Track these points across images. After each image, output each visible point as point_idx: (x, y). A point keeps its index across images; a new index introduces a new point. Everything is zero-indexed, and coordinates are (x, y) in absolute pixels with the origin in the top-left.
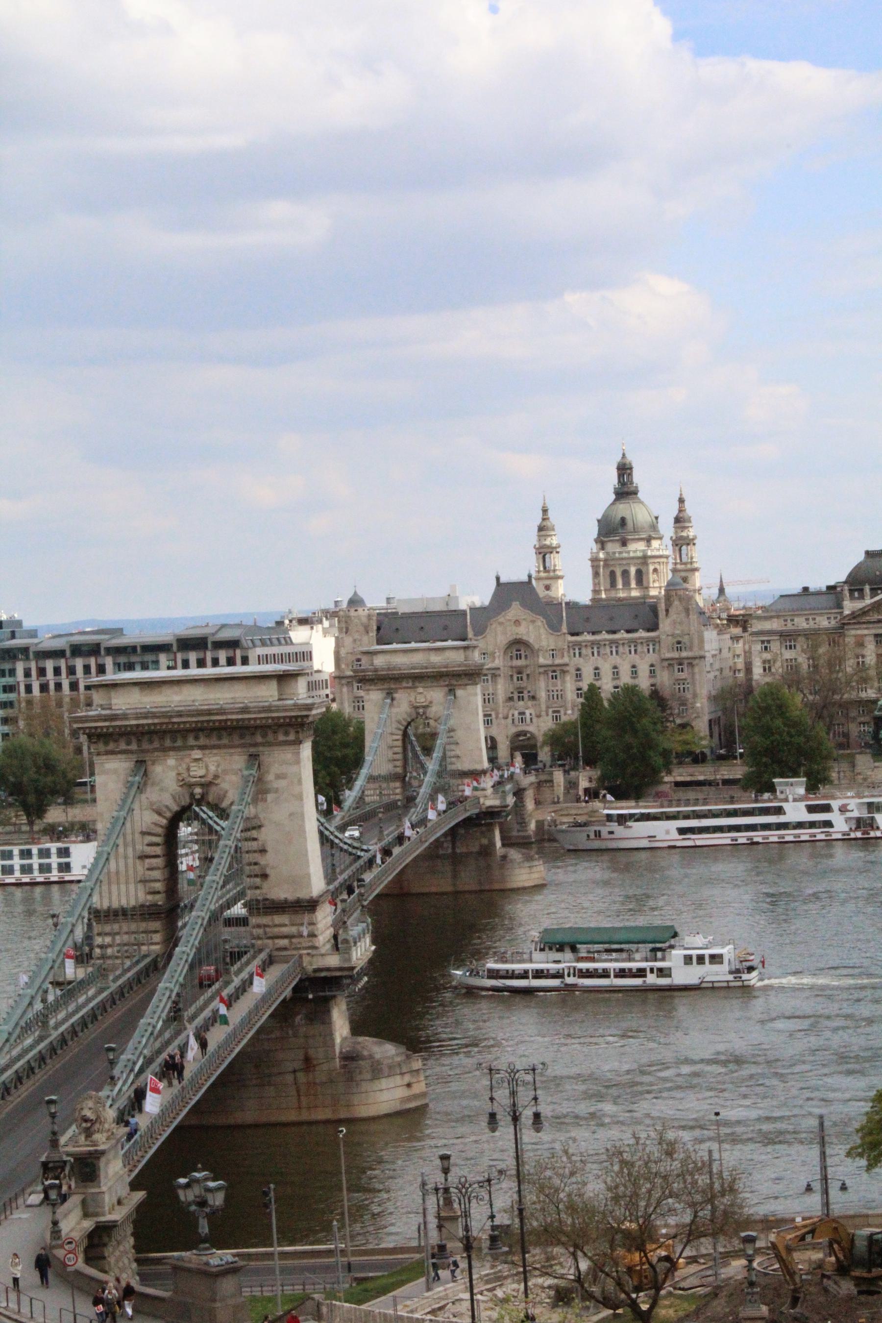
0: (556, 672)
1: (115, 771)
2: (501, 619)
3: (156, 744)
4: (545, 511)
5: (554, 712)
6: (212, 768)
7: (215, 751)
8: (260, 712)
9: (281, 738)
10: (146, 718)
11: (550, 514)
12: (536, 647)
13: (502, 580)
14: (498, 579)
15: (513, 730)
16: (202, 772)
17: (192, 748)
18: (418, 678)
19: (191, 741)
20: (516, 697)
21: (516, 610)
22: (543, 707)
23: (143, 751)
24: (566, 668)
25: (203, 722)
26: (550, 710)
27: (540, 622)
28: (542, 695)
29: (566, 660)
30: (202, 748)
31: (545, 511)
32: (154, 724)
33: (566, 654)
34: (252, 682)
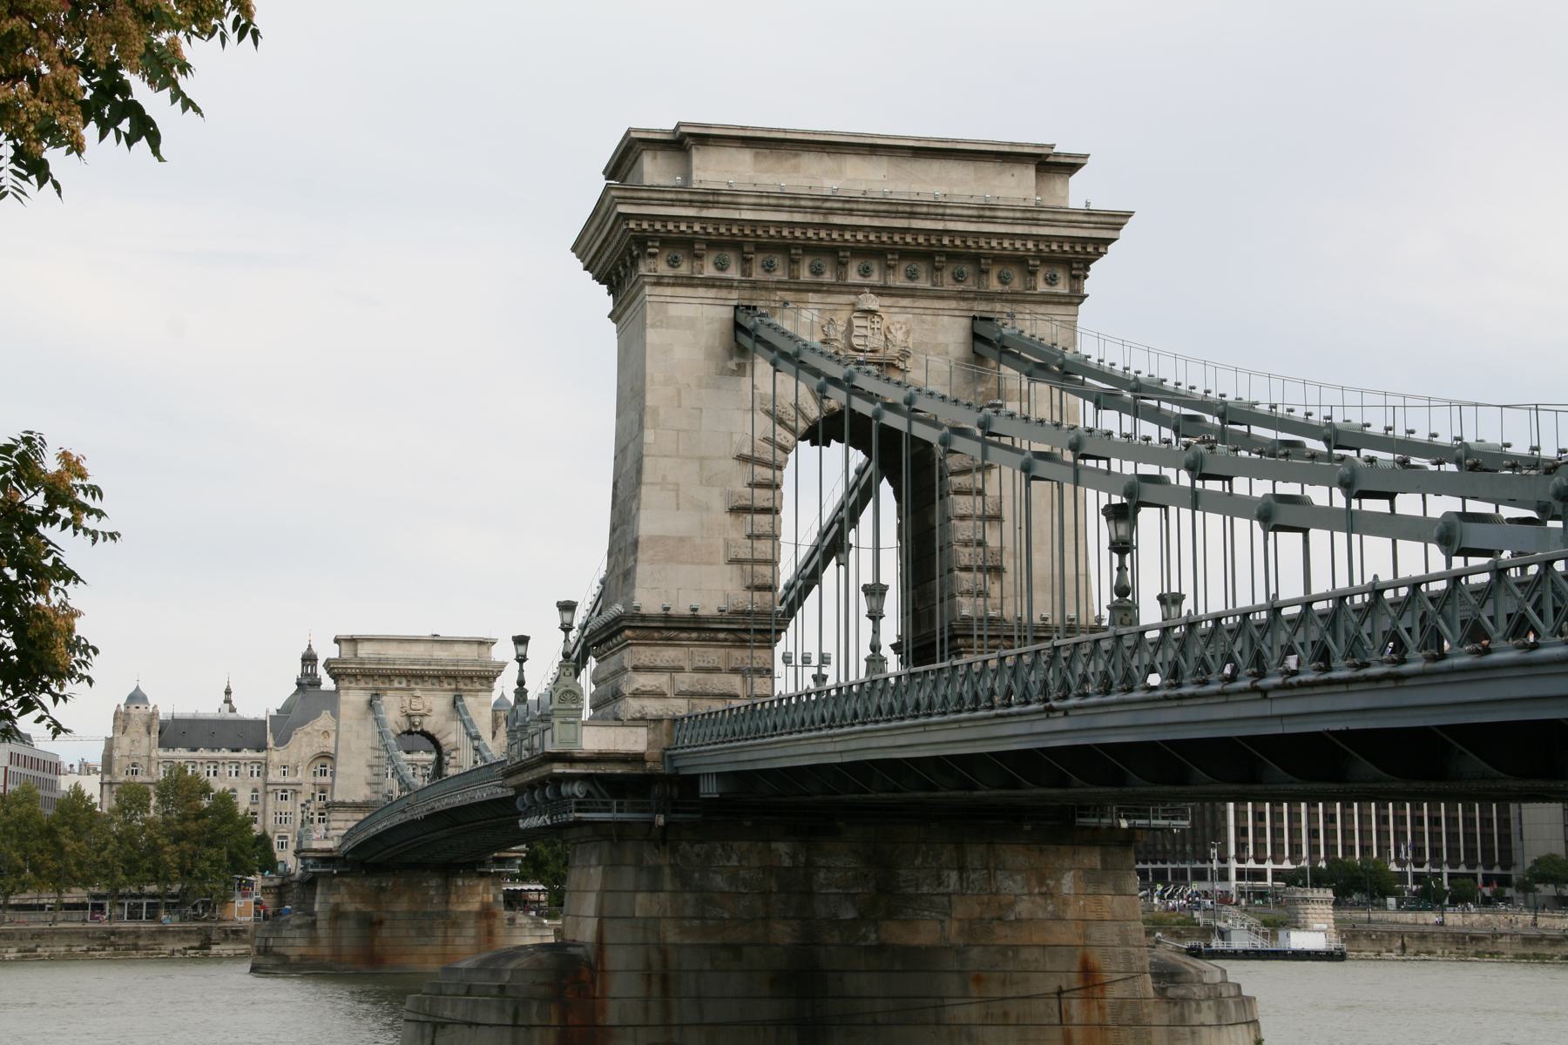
1: (690, 323)
2: (307, 728)
3: (780, 274)
4: (228, 692)
6: (898, 336)
7: (906, 302)
8: (1015, 221)
9: (1042, 287)
10: (777, 208)
11: (233, 697)
16: (876, 341)
17: (857, 289)
18: (415, 677)
19: (853, 277)
23: (755, 286)
25: (891, 230)
30: (882, 291)
31: (228, 692)
32: (792, 225)
34: (989, 168)
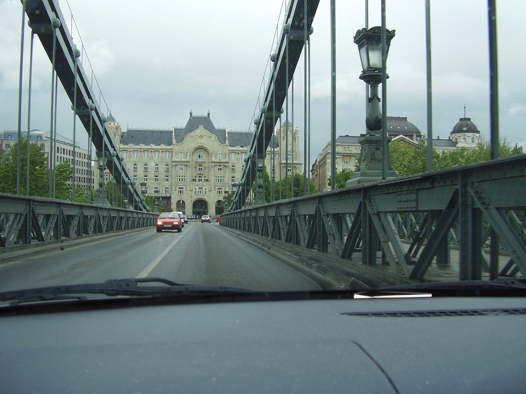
0: (221, 165)
2: (192, 134)
5: (218, 189)
12: (211, 151)
13: (194, 114)
14: (191, 114)
15: (195, 198)
20: (197, 180)
21: (201, 130)
22: (213, 186)
24: (226, 165)
26: (217, 188)
27: (214, 137)
28: (212, 179)
29: (227, 160)
33: (227, 156)
